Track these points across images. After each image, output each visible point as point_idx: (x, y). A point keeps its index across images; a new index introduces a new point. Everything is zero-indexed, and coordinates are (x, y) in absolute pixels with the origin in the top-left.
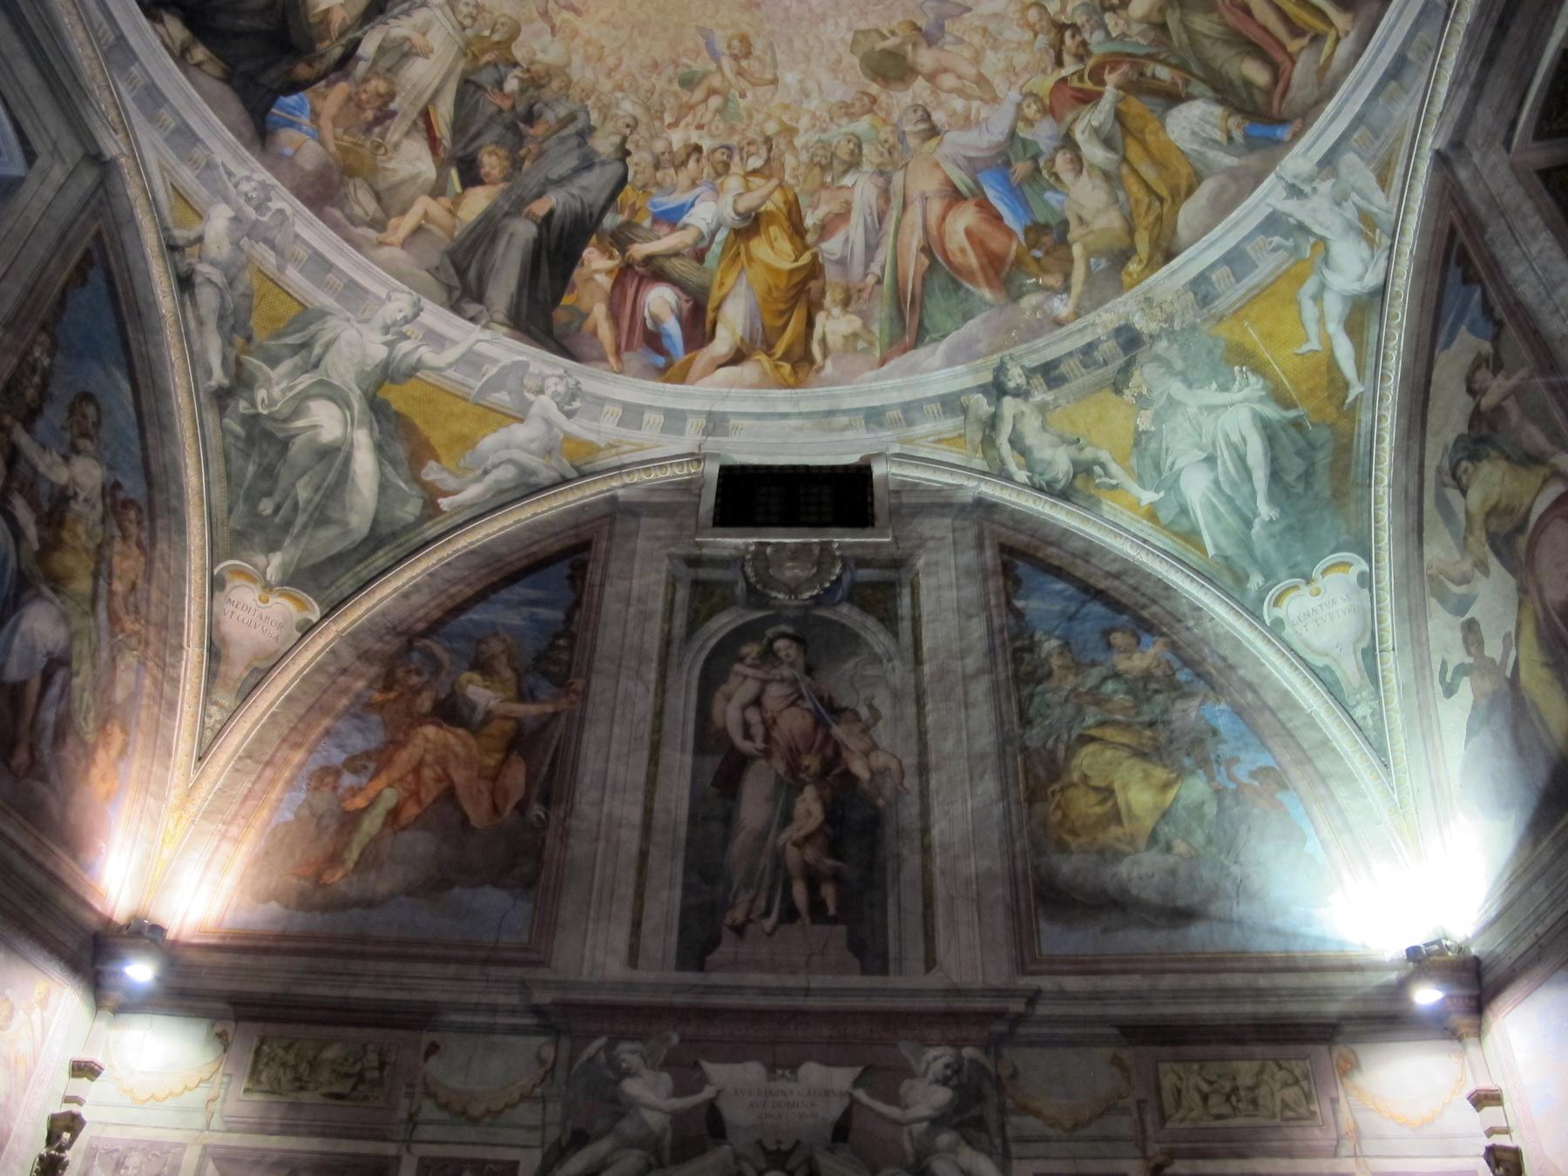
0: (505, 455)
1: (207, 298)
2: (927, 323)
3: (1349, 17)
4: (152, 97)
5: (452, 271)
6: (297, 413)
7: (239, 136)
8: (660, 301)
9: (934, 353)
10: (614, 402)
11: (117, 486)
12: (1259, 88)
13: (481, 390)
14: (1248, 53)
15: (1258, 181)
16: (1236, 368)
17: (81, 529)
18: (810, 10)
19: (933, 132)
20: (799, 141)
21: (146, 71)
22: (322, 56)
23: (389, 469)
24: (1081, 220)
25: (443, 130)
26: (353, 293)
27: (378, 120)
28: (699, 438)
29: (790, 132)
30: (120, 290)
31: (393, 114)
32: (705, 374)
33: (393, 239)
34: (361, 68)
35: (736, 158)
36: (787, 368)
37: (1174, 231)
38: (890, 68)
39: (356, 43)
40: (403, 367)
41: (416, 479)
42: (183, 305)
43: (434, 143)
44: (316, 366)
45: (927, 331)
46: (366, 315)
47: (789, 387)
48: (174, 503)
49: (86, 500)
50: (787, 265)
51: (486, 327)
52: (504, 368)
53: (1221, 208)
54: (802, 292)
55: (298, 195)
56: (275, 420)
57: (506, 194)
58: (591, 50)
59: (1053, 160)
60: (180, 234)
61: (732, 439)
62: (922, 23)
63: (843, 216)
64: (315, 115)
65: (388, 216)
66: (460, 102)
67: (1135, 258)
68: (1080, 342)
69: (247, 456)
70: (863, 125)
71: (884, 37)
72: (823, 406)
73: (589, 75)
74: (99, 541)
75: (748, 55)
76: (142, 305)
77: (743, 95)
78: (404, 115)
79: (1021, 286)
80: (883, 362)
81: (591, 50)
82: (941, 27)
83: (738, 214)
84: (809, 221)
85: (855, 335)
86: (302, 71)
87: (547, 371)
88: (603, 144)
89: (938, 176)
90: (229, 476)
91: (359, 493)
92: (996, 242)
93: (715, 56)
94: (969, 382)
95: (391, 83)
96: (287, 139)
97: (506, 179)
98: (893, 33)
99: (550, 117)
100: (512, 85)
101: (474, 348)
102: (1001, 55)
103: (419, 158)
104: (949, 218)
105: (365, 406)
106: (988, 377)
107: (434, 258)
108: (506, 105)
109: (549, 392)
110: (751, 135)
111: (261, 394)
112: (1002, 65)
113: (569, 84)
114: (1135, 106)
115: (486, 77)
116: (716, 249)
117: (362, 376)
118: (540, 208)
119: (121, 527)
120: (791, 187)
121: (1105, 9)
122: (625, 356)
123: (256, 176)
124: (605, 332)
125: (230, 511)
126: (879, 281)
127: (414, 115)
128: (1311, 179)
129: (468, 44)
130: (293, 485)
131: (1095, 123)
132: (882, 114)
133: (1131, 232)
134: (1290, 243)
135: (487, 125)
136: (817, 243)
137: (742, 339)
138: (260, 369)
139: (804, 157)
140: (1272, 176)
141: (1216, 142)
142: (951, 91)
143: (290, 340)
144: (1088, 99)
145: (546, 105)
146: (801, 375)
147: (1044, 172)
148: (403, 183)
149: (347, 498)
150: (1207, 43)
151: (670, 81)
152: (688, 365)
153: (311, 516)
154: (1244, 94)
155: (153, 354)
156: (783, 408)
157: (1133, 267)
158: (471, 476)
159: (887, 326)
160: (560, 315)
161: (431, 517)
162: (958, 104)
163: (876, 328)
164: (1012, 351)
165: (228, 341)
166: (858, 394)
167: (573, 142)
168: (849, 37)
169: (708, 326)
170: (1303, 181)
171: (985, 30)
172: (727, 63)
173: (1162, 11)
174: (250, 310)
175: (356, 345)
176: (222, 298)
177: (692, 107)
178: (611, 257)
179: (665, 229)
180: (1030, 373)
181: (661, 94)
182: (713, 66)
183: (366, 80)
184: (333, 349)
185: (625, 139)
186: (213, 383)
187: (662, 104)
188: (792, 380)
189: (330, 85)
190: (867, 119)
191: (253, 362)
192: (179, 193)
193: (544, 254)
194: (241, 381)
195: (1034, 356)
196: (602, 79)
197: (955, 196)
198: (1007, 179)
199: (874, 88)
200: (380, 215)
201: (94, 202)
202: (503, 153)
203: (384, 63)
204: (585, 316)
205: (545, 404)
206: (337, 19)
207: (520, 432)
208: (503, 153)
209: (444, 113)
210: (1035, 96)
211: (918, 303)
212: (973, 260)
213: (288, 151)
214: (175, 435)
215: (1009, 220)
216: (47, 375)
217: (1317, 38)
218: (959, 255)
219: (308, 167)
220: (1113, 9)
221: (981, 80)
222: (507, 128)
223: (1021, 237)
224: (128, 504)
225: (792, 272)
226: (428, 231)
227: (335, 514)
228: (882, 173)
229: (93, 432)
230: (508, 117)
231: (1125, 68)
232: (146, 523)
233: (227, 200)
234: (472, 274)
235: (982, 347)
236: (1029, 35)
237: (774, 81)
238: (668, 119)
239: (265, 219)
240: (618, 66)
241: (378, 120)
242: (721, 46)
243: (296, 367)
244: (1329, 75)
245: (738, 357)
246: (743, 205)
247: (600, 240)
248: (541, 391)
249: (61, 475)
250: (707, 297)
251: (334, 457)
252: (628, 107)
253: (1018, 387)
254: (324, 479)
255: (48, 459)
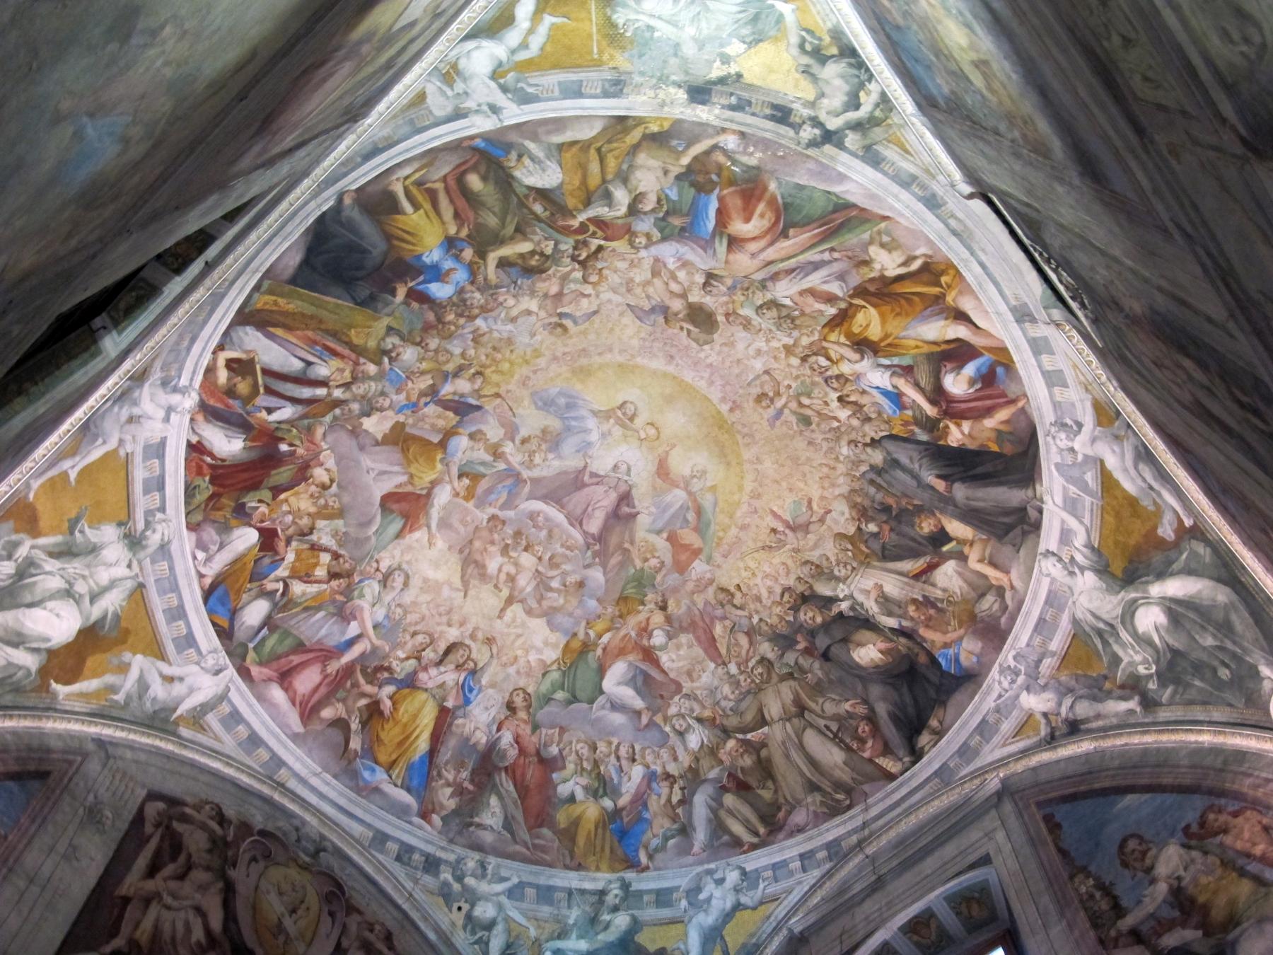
0: (1132, 471)
1: (1084, 709)
2: (830, 208)
3: (391, 188)
4: (966, 752)
5: (1011, 535)
6: (1150, 643)
7: (975, 693)
8: (957, 384)
9: (847, 192)
10: (1051, 396)
11: (1187, 829)
12: (478, 173)
13: (1091, 496)
14: (472, 192)
15: (518, 126)
16: (628, 34)
17: (1204, 880)
18: (712, 374)
19: (710, 277)
20: (791, 342)
21: (952, 756)
22: (909, 648)
23: (1175, 567)
24: (666, 172)
25: (919, 564)
26: (1055, 601)
27: (933, 605)
28: (1040, 324)
29: (789, 350)
30: (1072, 790)
31: (924, 596)
32: (988, 334)
33: (1006, 580)
34: (905, 623)
35: (829, 373)
36: (944, 279)
37: (605, 129)
38: (701, 319)
39: (892, 629)
40: (1095, 559)
41: (1176, 545)
42: (1090, 731)
43: (931, 567)
44: (1112, 626)
45: (836, 205)
46: (1066, 589)
47: (958, 272)
48: (1218, 763)
49: (1186, 869)
50: (872, 310)
51: (1042, 501)
52: (1067, 481)
53: (559, 124)
54: (881, 292)
55: (1001, 649)
56: (1159, 659)
57: (942, 512)
58: (826, 485)
59: (653, 210)
60: (1044, 731)
61: (1026, 300)
62: (661, 319)
63: (811, 292)
64: (946, 645)
65: (991, 586)
66: (899, 558)
67: (647, 131)
68: (738, 116)
69: (1188, 686)
70: (747, 312)
71: (689, 332)
72: (954, 241)
73: (841, 480)
74: (1218, 862)
75: (764, 395)
76: (1085, 769)
77: (789, 387)
78: (923, 590)
79: (744, 172)
80: (885, 218)
81: (826, 485)
82: (653, 310)
83: (863, 358)
84: (832, 311)
85: (883, 245)
86: (923, 659)
87: (1054, 449)
88: (877, 457)
89: (731, 257)
90: (1204, 703)
91: (1200, 592)
92: (735, 203)
93: (780, 413)
94: (844, 157)
95: (907, 604)
96: (967, 660)
97: (934, 515)
98: (682, 328)
99: (879, 497)
100: (872, 527)
101: (1063, 510)
102: (632, 274)
103: (946, 574)
104: (751, 236)
105: (1131, 588)
106: (828, 148)
107: (1007, 550)
108: (886, 528)
109: (1070, 444)
110: (808, 372)
111: (1142, 670)
112: (636, 270)
113: (853, 491)
114: (571, 202)
115: (876, 546)
116: (896, 361)
117: (1110, 590)
118: (940, 485)
119: (1216, 834)
120: (820, 332)
121: (547, 257)
122: (1012, 396)
123: (997, 677)
124: (1003, 414)
125: (1231, 705)
126: (832, 250)
127: (920, 584)
128: (477, 111)
129: (862, 563)
130: (1204, 648)
131: (606, 209)
132: (730, 306)
133: (636, 148)
134: (520, 85)
135: (903, 535)
136: (841, 299)
137: (946, 319)
138: (1124, 670)
139: (796, 333)
140: (506, 123)
141: (532, 160)
142: (679, 283)
143: (1100, 646)
144: (599, 223)
145: (873, 502)
146: (943, 267)
147: (665, 208)
148: (966, 581)
149: (1205, 603)
150: (496, 209)
151: (813, 431)
152: (990, 350)
153: (1226, 636)
154: (492, 174)
155: (1116, 763)
156: (978, 269)
157: (654, 128)
158: (1158, 500)
159: (858, 231)
160: (1008, 449)
161: (1203, 533)
162: (681, 275)
163: (866, 236)
164: (793, 147)
165: (1109, 695)
166: (925, 222)
167: (887, 476)
168: (706, 347)
169: (952, 346)
170: (485, 112)
171: (629, 291)
172: (779, 403)
173: (512, 238)
174: (1085, 676)
175: (1090, 596)
176: (1081, 697)
177: (819, 413)
178: (947, 427)
179: (905, 399)
180: (797, 127)
181: (825, 433)
182: (786, 411)
183: (912, 619)
184: (1098, 613)
185: (866, 445)
186: (1138, 710)
187: (830, 431)
188: (952, 272)
189: (925, 640)
190: (741, 312)
191: (1120, 675)
192: (1019, 732)
193: (971, 473)
194: (1133, 686)
195: (781, 132)
196: (839, 472)
197: (734, 243)
198: (692, 224)
199: (721, 318)
200: (993, 592)
201: (1021, 804)
202: (917, 520)
203: (896, 610)
204: (999, 432)
205: (1081, 444)
206: (883, 646)
207: (1112, 462)
208: (917, 520)
209: (908, 566)
210: (631, 244)
211: (822, 220)
212: (761, 207)
213: (974, 659)
214: (1173, 748)
215: (713, 205)
216: (1101, 886)
217: (419, 184)
218: (767, 216)
219: (980, 644)
220: (542, 254)
221: (655, 273)
222: (900, 522)
223: (717, 191)
224: (1202, 824)
225: (874, 306)
226: (991, 556)
227: (1219, 616)
228: (764, 287)
229: (1144, 847)
230: (893, 524)
231: (561, 223)
232: (1223, 801)
233: (1017, 696)
234: (1006, 520)
235: (811, 165)
236: (605, 272)
237: (767, 372)
238: (836, 424)
239: (1023, 668)
240: (826, 465)
241: (933, 605)
242: (771, 412)
243: (1116, 642)
244: (424, 161)
245: (961, 317)
246: (857, 356)
247: (940, 438)
248: (1072, 450)
249: (1162, 888)
250: (932, 353)
251: (1176, 610)
252: (845, 450)
253: (813, 127)
254: (1195, 622)
255: (1147, 900)
